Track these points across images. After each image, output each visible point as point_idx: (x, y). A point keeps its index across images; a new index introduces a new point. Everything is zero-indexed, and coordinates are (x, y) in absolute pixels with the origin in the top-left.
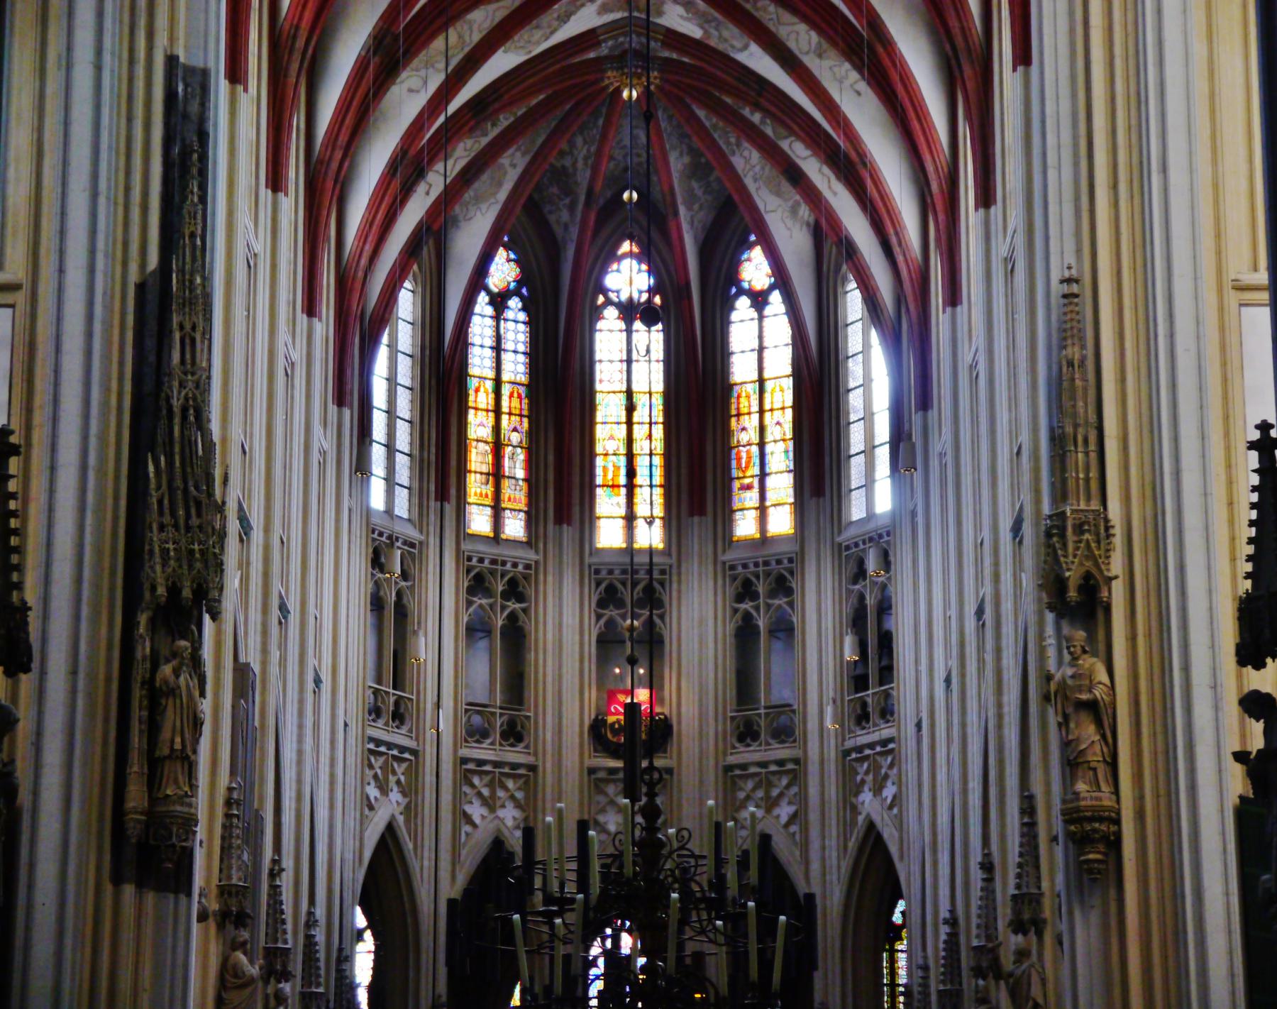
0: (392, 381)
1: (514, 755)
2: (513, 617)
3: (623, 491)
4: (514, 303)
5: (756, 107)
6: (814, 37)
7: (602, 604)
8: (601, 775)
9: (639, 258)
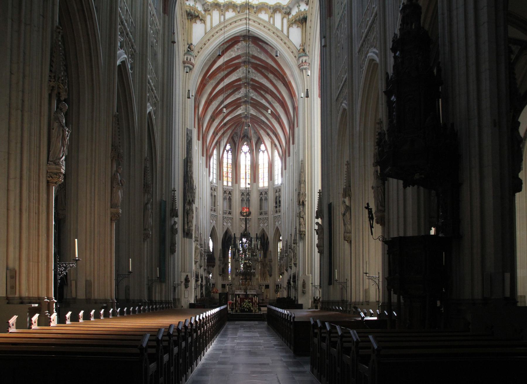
0: (213, 163)
1: (230, 216)
2: (230, 197)
3: (245, 179)
4: (230, 152)
5: (263, 125)
6: (271, 116)
7: (242, 195)
8: (242, 219)
9: (247, 145)
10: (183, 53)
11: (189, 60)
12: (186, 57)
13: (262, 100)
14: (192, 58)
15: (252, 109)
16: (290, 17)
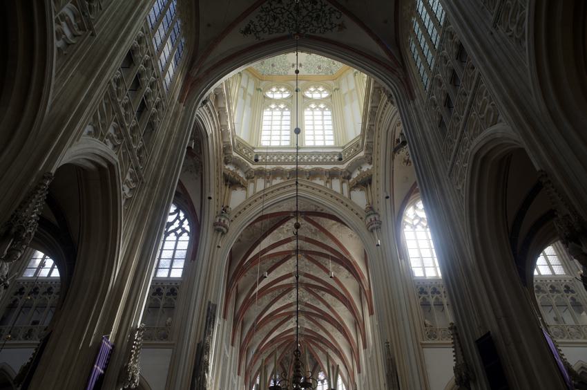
10: (216, 215)
11: (222, 221)
12: (218, 218)
13: (319, 304)
14: (227, 221)
15: (307, 322)
16: (351, 181)
